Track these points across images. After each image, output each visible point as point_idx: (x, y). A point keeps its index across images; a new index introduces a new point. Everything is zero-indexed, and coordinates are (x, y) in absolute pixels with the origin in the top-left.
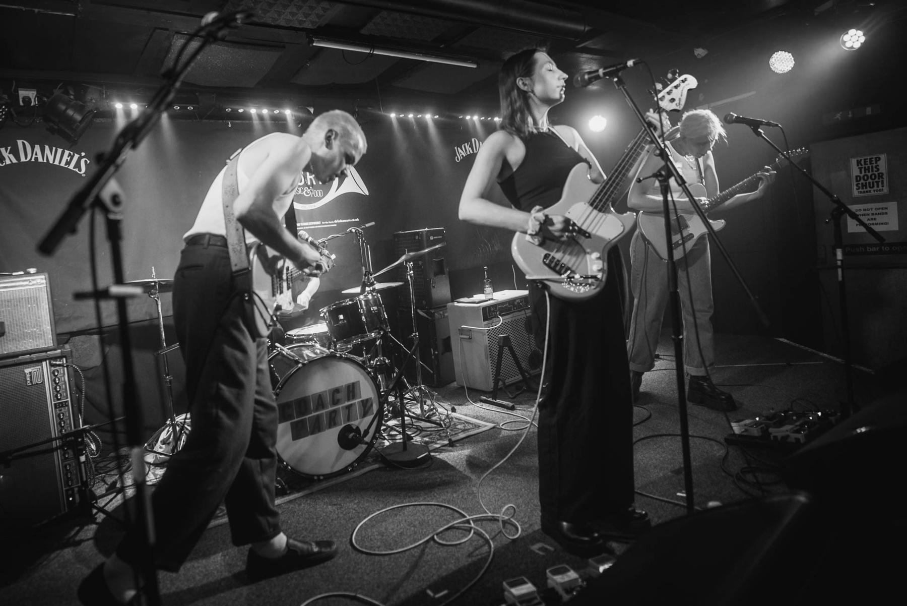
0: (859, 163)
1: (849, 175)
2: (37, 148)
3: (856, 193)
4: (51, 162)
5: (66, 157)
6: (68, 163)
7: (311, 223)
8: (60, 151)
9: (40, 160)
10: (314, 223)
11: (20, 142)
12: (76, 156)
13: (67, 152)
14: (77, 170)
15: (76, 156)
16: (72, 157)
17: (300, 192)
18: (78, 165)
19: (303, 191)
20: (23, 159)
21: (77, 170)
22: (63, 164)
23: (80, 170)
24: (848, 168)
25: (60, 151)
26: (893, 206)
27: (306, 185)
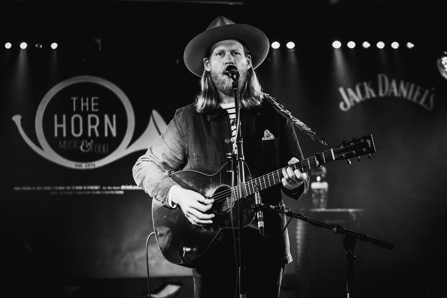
7: (85, 188)
17: (75, 146)
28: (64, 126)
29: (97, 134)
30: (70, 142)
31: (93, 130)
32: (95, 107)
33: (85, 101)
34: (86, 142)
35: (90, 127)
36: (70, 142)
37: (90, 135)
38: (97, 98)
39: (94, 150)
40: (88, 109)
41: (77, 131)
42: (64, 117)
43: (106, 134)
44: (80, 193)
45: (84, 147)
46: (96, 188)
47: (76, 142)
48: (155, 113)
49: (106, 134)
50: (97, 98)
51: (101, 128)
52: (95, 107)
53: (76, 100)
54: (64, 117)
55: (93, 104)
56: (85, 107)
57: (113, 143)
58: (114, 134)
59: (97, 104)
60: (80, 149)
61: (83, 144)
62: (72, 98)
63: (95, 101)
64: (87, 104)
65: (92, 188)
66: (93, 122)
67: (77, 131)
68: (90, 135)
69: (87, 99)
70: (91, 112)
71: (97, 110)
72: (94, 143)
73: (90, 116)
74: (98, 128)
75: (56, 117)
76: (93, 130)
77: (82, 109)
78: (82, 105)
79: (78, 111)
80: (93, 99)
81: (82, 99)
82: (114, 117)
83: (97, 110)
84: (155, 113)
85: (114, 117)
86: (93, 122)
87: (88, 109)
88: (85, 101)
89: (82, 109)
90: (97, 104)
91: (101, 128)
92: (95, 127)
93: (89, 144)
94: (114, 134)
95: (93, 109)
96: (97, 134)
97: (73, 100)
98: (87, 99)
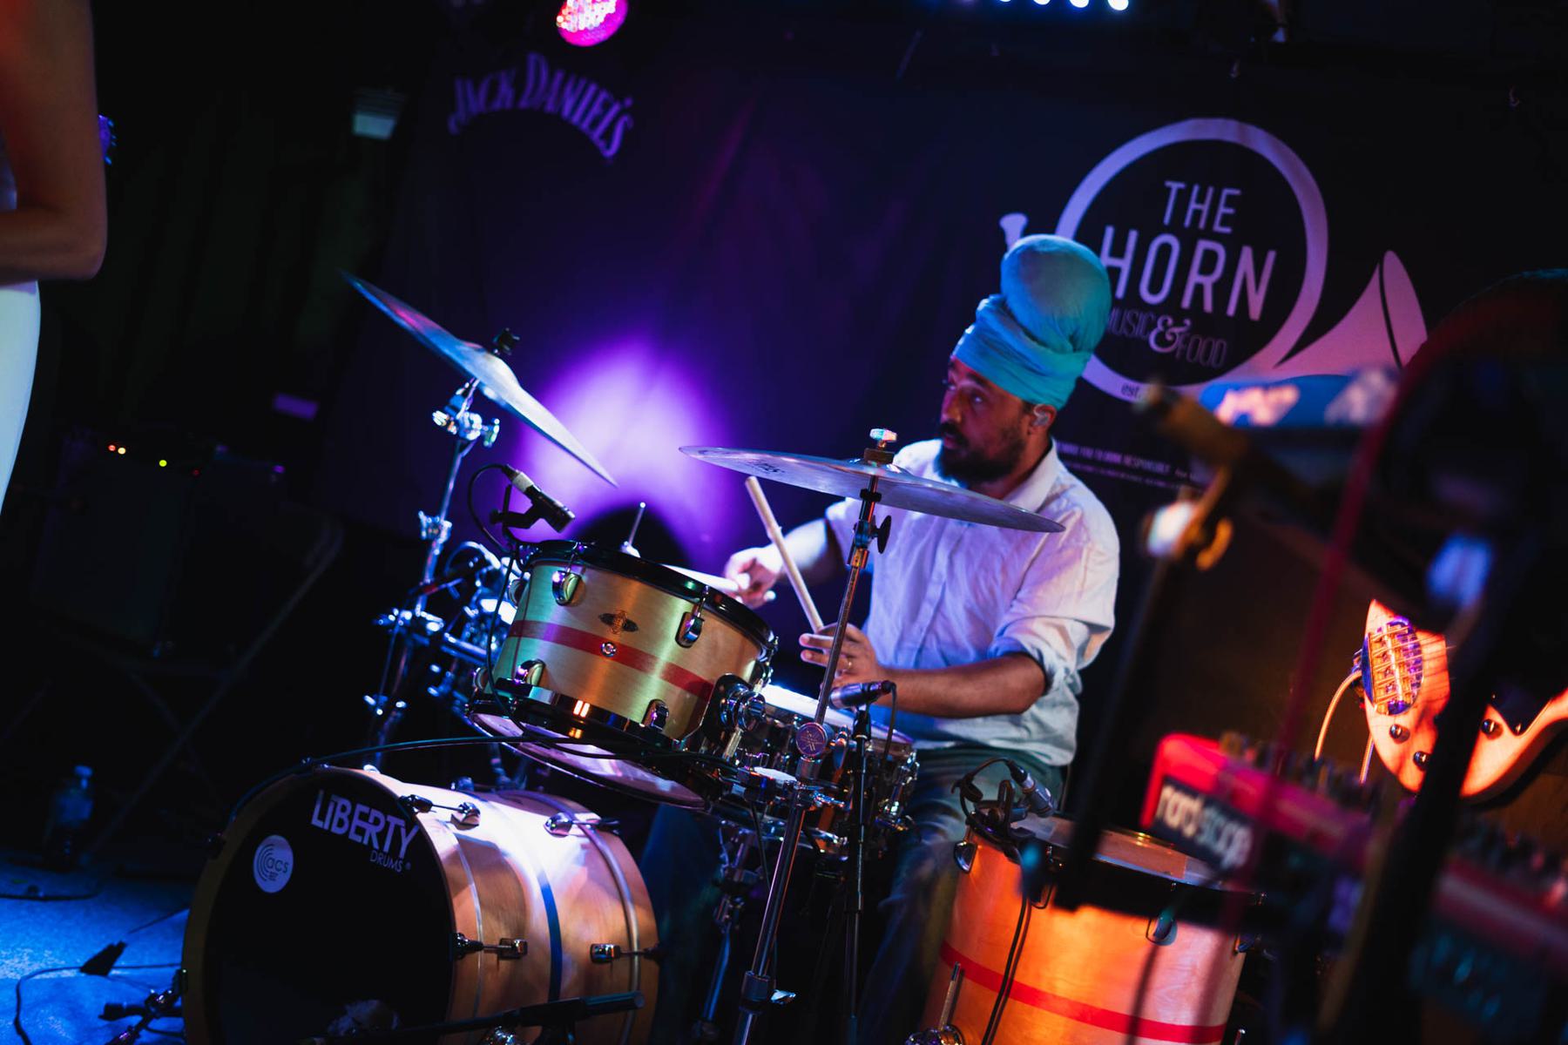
2: (559, 76)
4: (566, 113)
5: (596, 110)
6: (595, 123)
7: (1128, 460)
8: (592, 88)
9: (549, 108)
10: (1148, 465)
11: (533, 58)
12: (616, 108)
13: (603, 96)
14: (601, 144)
15: (616, 108)
16: (606, 107)
17: (1138, 331)
18: (608, 136)
19: (1151, 325)
20: (523, 104)
21: (601, 144)
22: (585, 126)
23: (609, 146)
25: (592, 88)
27: (1171, 306)
28: (1125, 265)
29: (1208, 306)
30: (1128, 316)
31: (1199, 288)
32: (1226, 220)
33: (1201, 200)
34: (1170, 321)
35: (1194, 278)
36: (1128, 316)
37: (1186, 302)
38: (1237, 192)
39: (1184, 352)
40: (1202, 225)
41: (1155, 287)
42: (1133, 236)
43: (1231, 311)
44: (1111, 473)
45: (1161, 339)
46: (1160, 468)
47: (1143, 318)
48: (1393, 266)
49: (1231, 311)
50: (1237, 192)
51: (1222, 289)
52: (1226, 220)
53: (1179, 191)
54: (1133, 236)
55: (1222, 210)
56: (1197, 213)
58: (1255, 311)
59: (1230, 211)
60: (1147, 343)
61: (1160, 327)
62: (1168, 184)
63: (1231, 201)
64: (1205, 208)
65: (1148, 465)
66: (1207, 268)
67: (1155, 287)
68: (1186, 302)
70: (1210, 234)
71: (1227, 230)
72: (1192, 331)
73: (1203, 245)
74: (1216, 286)
75: (1109, 232)
76: (1199, 288)
77: (1187, 223)
78: (1193, 206)
79: (1175, 228)
81: (1196, 189)
82: (1271, 256)
83: (1227, 230)
84: (1392, 261)
85: (1271, 256)
86: (1207, 268)
87: (1202, 225)
88: (1201, 200)
89: (1187, 223)
90: (1230, 211)
91: (1222, 289)
92: (1208, 282)
93: (1176, 330)
94: (1255, 311)
95: (1217, 228)
96: (1208, 306)
97: (1169, 189)
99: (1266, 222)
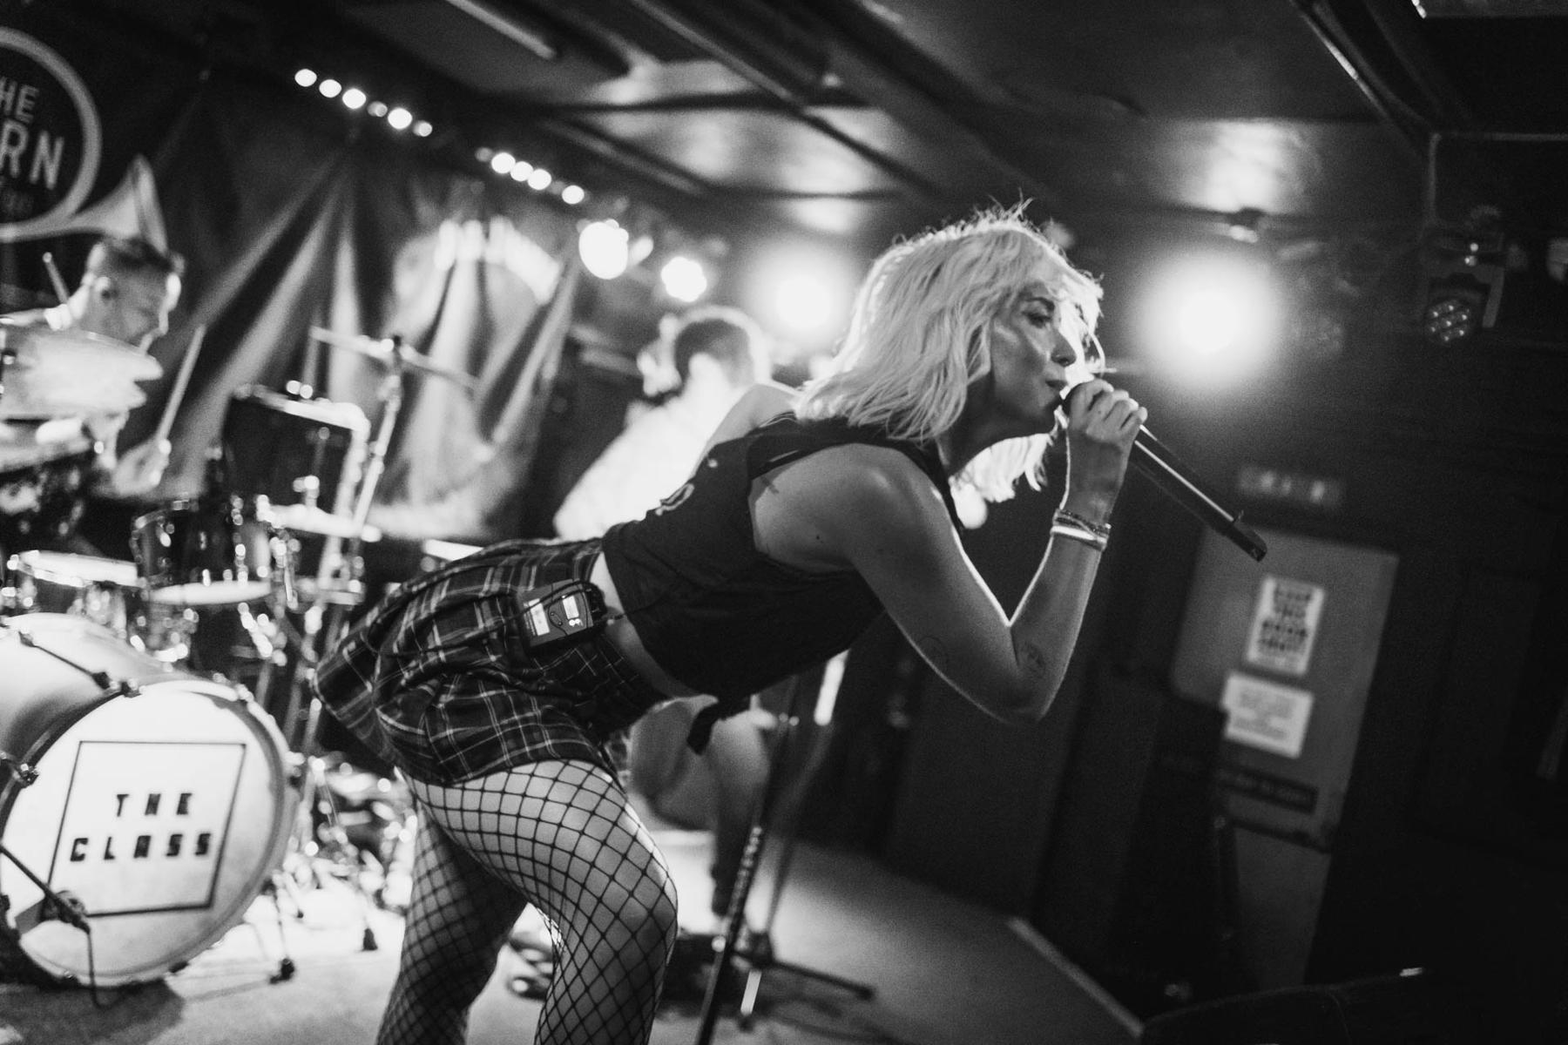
0: (1277, 593)
1: (1251, 612)
3: (1254, 654)
24: (1254, 595)
26: (1301, 704)
32: (25, 111)
40: (8, 108)
49: (35, 175)
50: (34, 91)
51: (27, 159)
52: (25, 111)
55: (22, 103)
57: (42, 200)
63: (28, 97)
69: (12, 88)
70: (12, 117)
80: (24, 91)
83: (26, 118)
85: (59, 146)
91: (27, 159)
92: (15, 153)
95: (19, 112)
96: (15, 169)
98: (12, 88)
99: (53, 114)
